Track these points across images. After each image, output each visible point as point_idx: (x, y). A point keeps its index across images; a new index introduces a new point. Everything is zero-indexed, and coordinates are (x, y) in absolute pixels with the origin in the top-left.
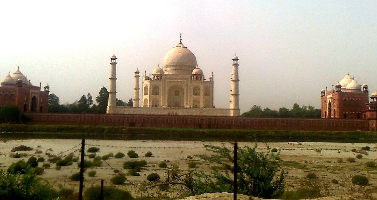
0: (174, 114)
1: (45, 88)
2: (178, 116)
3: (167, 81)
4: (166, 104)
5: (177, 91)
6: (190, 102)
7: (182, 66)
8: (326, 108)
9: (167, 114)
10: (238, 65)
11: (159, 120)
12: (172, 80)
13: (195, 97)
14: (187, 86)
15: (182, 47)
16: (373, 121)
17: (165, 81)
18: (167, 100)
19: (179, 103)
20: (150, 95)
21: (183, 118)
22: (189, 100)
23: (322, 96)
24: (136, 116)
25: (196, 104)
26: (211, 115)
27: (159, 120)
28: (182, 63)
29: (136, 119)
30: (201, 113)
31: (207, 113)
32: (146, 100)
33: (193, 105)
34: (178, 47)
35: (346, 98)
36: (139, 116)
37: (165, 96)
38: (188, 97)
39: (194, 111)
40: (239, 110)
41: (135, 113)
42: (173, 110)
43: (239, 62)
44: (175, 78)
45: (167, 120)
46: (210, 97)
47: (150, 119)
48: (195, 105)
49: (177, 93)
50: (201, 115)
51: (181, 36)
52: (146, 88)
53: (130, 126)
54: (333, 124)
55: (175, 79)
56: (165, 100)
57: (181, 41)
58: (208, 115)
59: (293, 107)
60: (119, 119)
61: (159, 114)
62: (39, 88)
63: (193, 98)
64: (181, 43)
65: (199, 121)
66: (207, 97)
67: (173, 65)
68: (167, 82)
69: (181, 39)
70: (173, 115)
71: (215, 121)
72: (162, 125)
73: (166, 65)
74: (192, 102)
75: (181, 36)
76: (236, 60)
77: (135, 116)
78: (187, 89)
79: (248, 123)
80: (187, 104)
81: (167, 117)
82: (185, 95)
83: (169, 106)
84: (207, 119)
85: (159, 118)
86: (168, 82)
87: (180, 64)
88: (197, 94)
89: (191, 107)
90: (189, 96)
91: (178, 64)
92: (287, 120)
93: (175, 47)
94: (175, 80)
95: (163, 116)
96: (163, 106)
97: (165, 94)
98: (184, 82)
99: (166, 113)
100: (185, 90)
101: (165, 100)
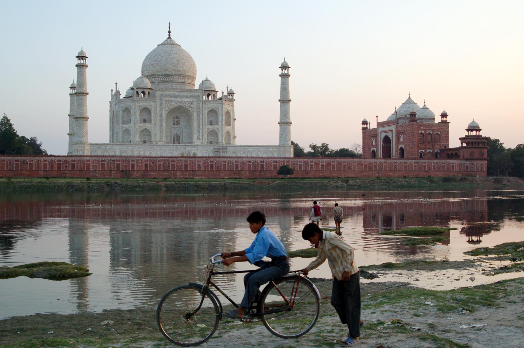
3: (165, 99)
4: (164, 140)
8: (377, 144)
9: (180, 155)
10: (289, 76)
11: (173, 165)
12: (172, 99)
14: (198, 108)
17: (161, 99)
18: (165, 132)
19: (181, 137)
20: (135, 124)
22: (201, 132)
23: (364, 129)
24: (133, 159)
26: (249, 155)
27: (173, 165)
28: (179, 71)
29: (133, 165)
30: (234, 153)
36: (137, 158)
37: (161, 125)
38: (199, 127)
41: (124, 154)
42: (189, 148)
44: (179, 96)
45: (186, 165)
50: (234, 155)
51: (169, 27)
53: (122, 177)
54: (425, 166)
56: (161, 132)
57: (169, 35)
58: (244, 156)
59: (314, 147)
60: (102, 164)
61: (165, 154)
64: (169, 38)
65: (237, 166)
67: (165, 74)
68: (164, 102)
69: (169, 32)
70: (190, 157)
71: (262, 166)
72: (178, 173)
73: (149, 74)
74: (205, 136)
75: (169, 27)
77: (130, 159)
78: (198, 115)
79: (311, 168)
82: (195, 125)
84: (250, 162)
85: (172, 161)
86: (167, 101)
87: (177, 73)
88: (211, 123)
90: (201, 127)
91: (174, 73)
92: (365, 162)
94: (179, 99)
95: (179, 159)
100: (195, 116)
101: (161, 132)
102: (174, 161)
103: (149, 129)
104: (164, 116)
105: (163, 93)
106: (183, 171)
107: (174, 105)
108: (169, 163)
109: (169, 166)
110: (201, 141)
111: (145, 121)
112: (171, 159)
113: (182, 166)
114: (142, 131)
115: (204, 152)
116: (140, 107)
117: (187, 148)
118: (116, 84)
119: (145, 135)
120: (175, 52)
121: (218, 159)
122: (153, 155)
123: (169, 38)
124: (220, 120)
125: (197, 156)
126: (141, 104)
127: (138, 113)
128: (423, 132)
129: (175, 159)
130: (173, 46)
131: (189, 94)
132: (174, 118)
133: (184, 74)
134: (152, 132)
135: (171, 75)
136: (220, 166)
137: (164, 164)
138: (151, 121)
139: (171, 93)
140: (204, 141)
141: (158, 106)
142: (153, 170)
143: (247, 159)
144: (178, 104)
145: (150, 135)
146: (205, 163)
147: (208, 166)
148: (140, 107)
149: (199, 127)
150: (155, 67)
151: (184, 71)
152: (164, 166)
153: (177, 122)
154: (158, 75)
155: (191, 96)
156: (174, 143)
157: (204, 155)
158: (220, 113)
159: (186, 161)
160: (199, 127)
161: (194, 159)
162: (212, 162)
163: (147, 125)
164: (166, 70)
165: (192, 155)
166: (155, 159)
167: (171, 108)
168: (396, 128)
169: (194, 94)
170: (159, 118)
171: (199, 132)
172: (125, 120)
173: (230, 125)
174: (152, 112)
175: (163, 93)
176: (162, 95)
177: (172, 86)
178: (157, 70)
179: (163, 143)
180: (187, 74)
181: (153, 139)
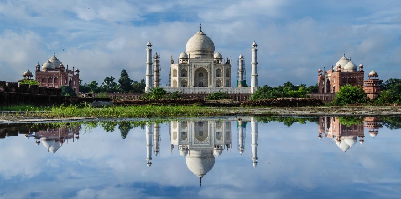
0: (203, 93)
1: (76, 72)
4: (193, 85)
8: (324, 85)
12: (197, 64)
16: (371, 95)
20: (179, 77)
32: (175, 82)
35: (345, 76)
40: (259, 87)
49: (201, 75)
52: (175, 71)
62: (72, 72)
69: (201, 27)
74: (215, 83)
80: (211, 84)
88: (218, 75)
94: (201, 64)
98: (208, 65)
107: (199, 67)
128: (346, 77)
168: (332, 75)
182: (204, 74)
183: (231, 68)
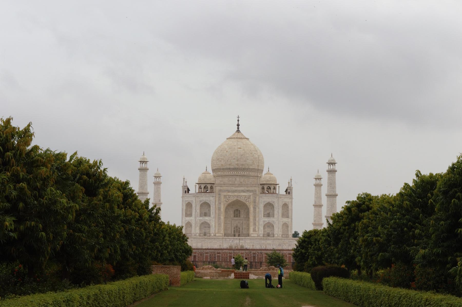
2: (247, 249)
4: (222, 232)
5: (237, 210)
6: (258, 228)
7: (244, 169)
10: (336, 171)
12: (230, 194)
13: (267, 220)
15: (241, 138)
17: (219, 194)
18: (222, 224)
19: (241, 229)
20: (195, 217)
21: (254, 254)
22: (257, 224)
25: (268, 230)
28: (242, 165)
31: (290, 245)
33: (264, 232)
34: (234, 138)
37: (219, 218)
39: (269, 242)
43: (337, 167)
46: (290, 220)
47: (205, 255)
48: (265, 233)
50: (280, 248)
51: (238, 121)
55: (235, 191)
56: (219, 224)
57: (238, 128)
63: (264, 221)
64: (238, 131)
66: (285, 220)
67: (229, 169)
68: (222, 197)
69: (238, 125)
73: (216, 168)
74: (261, 228)
75: (238, 121)
76: (332, 163)
78: (255, 208)
81: (230, 251)
83: (226, 235)
85: (218, 253)
86: (225, 196)
87: (241, 167)
88: (268, 215)
89: (261, 235)
90: (257, 219)
91: (237, 167)
93: (230, 138)
94: (236, 194)
95: (224, 251)
96: (217, 235)
97: (219, 215)
99: (225, 246)
100: (251, 209)
101: (219, 224)
102: (219, 253)
103: (208, 222)
104: (223, 209)
105: (222, 188)
106: (228, 262)
107: (232, 199)
108: (215, 255)
109: (215, 257)
110: (257, 233)
111: (205, 215)
112: (216, 251)
113: (227, 258)
114: (202, 223)
115: (252, 244)
116: (200, 201)
117: (235, 241)
118: (184, 179)
119: (206, 227)
120: (239, 147)
121: (260, 251)
122: (204, 248)
123: (238, 131)
124: (276, 212)
125: (245, 248)
126: (201, 199)
127: (198, 207)
129: (220, 251)
130: (239, 140)
131: (246, 189)
132: (235, 211)
133: (247, 167)
134: (211, 225)
135: (234, 169)
136: (262, 258)
137: (211, 255)
138: (210, 214)
139: (229, 188)
140: (260, 233)
141: (217, 200)
142: (201, 261)
143: (288, 252)
144: (235, 199)
145: (210, 227)
146: (248, 255)
147: (251, 258)
148: (200, 201)
149: (255, 220)
150: (221, 161)
151: (248, 164)
152: (211, 257)
153: (237, 213)
154: (223, 169)
155: (248, 191)
156: (235, 236)
157: (251, 248)
158: (276, 205)
159: (231, 253)
160: (255, 220)
161: (237, 251)
162: (255, 254)
163: (207, 219)
164: (230, 165)
165: (239, 248)
166: (202, 251)
167: (228, 203)
169: (251, 189)
170: (217, 212)
171: (255, 224)
172: (188, 213)
173: (288, 217)
174: (211, 206)
175: (222, 188)
176: (220, 190)
177: (236, 179)
178: (222, 165)
179: (221, 235)
180: (251, 167)
181: (212, 231)
182: (242, 212)
183: (292, 202)
